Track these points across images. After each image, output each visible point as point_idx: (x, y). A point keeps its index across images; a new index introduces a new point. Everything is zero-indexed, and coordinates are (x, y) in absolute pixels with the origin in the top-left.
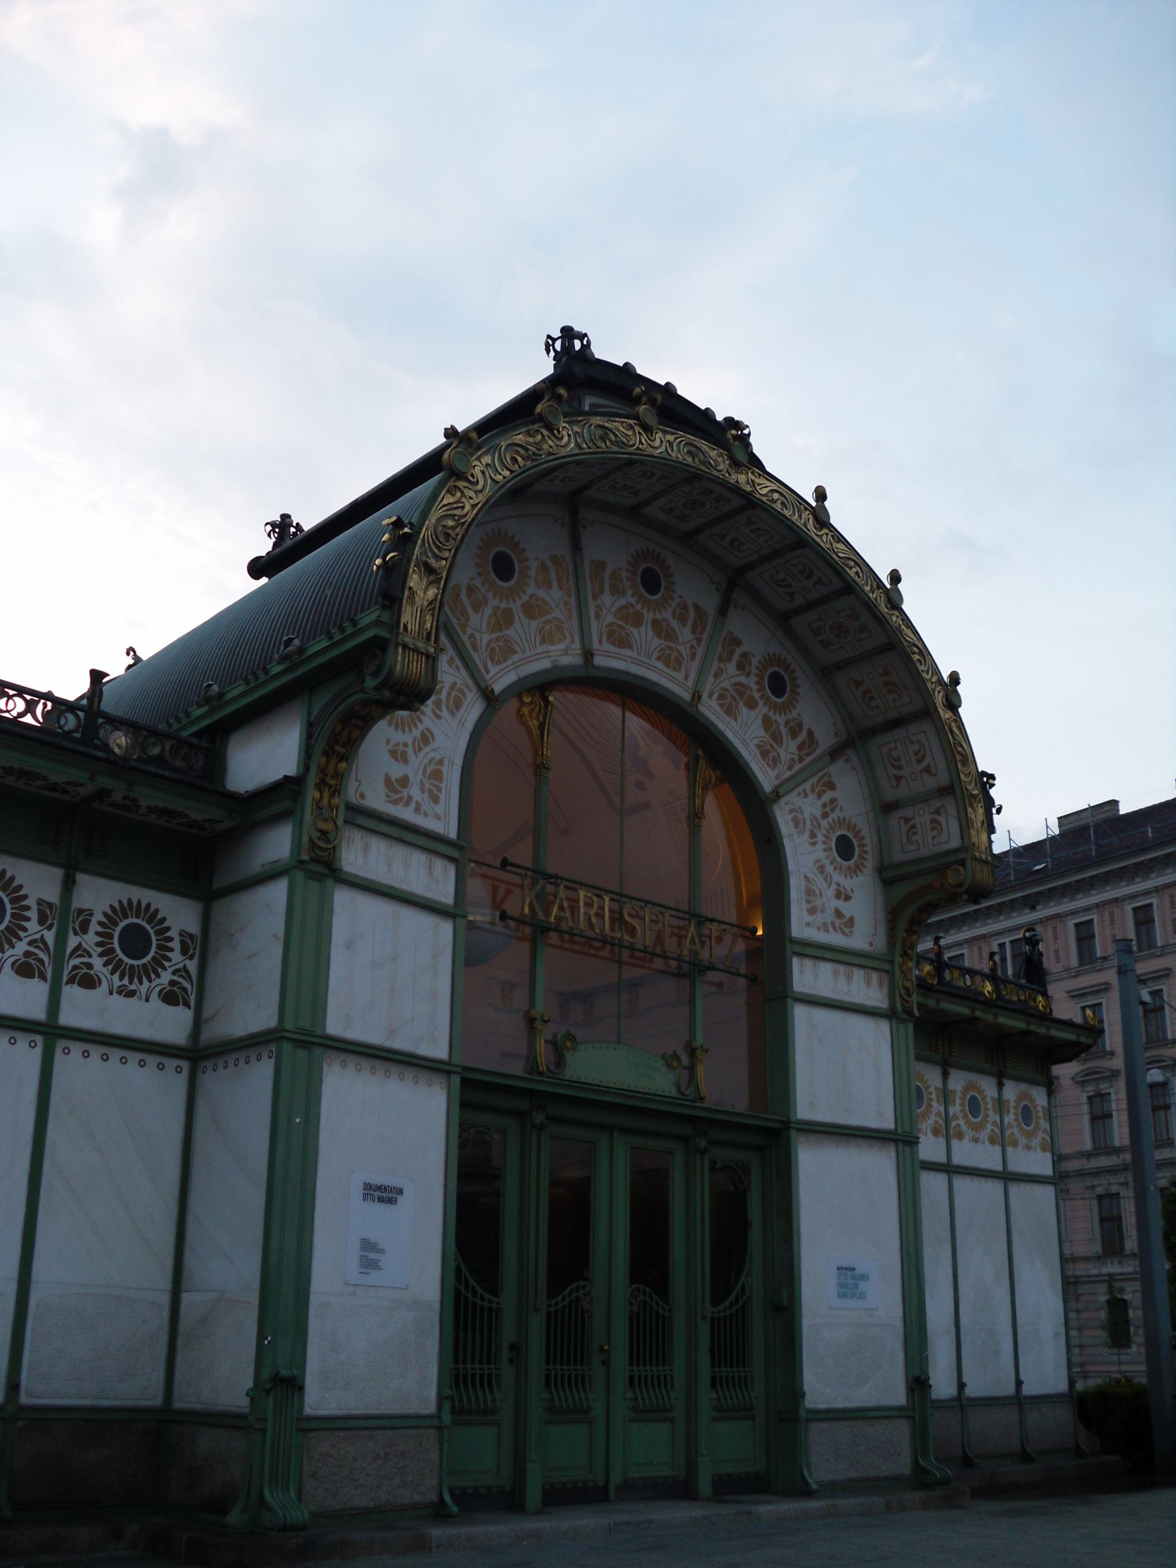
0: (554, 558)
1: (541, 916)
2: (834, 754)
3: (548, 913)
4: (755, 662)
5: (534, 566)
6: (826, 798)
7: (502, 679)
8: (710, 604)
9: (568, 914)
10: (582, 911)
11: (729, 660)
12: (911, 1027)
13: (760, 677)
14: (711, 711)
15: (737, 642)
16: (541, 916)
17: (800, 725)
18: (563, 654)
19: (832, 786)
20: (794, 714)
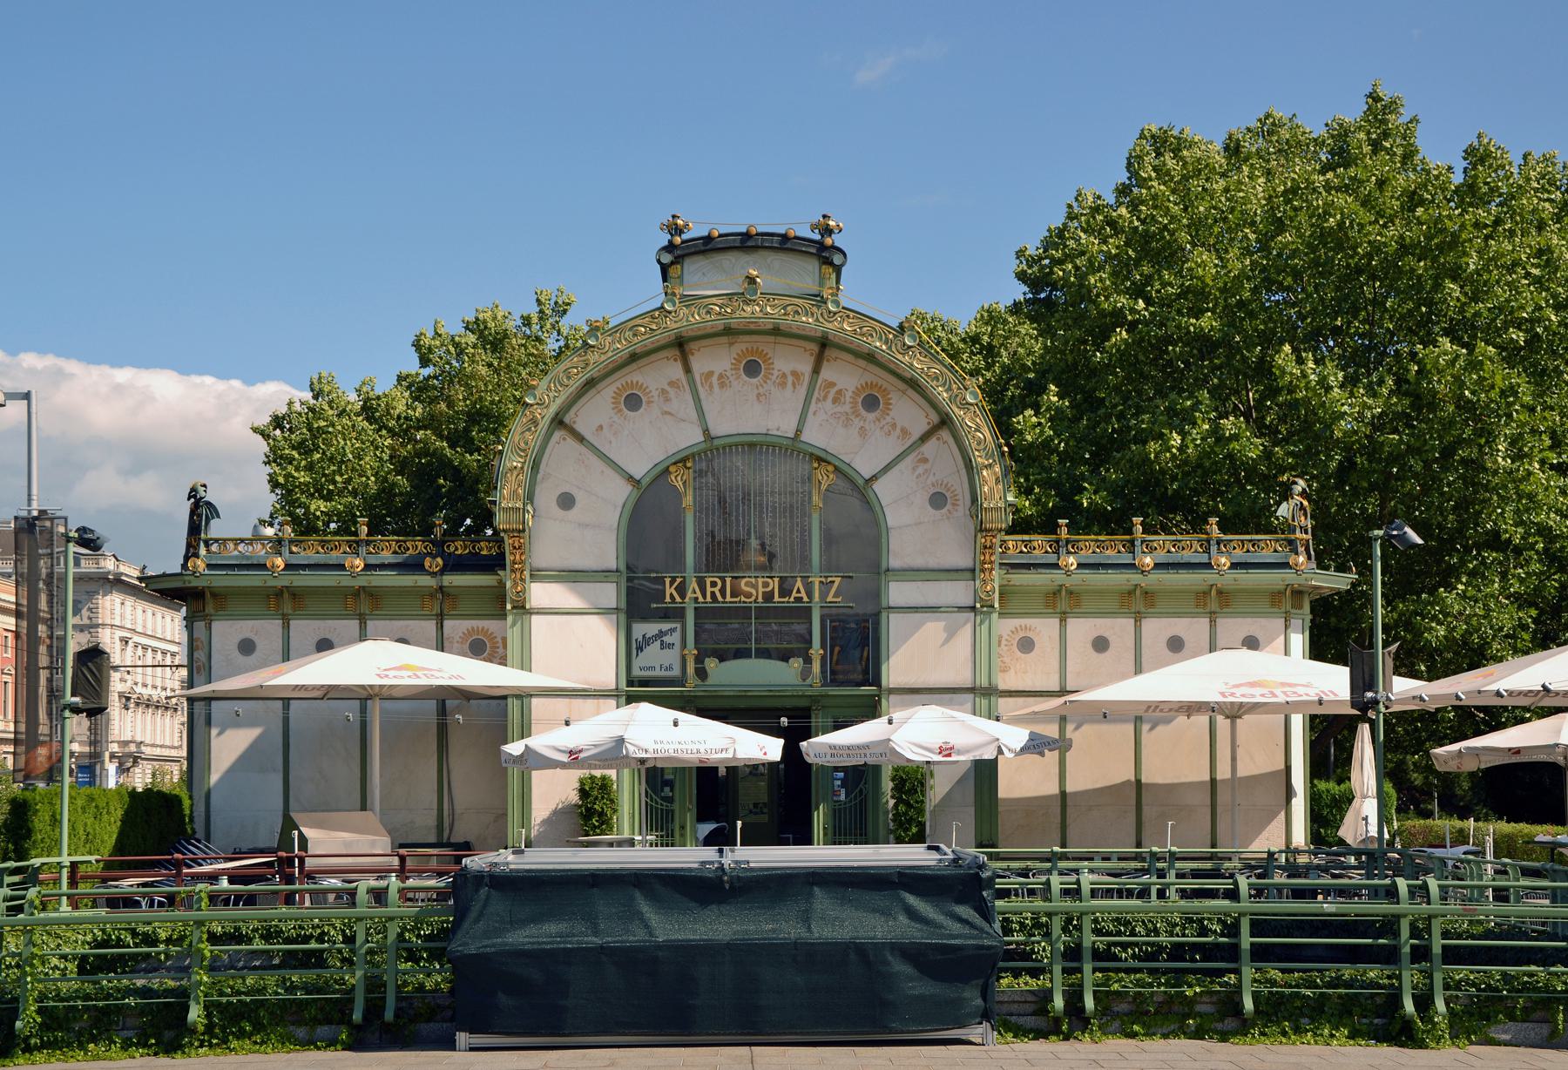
0: (671, 384)
1: (678, 599)
2: (924, 438)
3: (683, 596)
4: (849, 394)
5: (655, 393)
6: (920, 470)
7: (640, 468)
8: (806, 368)
9: (699, 594)
10: (709, 589)
11: (825, 398)
12: (995, 616)
13: (854, 403)
14: (814, 436)
15: (833, 384)
16: (678, 599)
17: (894, 426)
18: (690, 437)
19: (925, 460)
20: (888, 419)
